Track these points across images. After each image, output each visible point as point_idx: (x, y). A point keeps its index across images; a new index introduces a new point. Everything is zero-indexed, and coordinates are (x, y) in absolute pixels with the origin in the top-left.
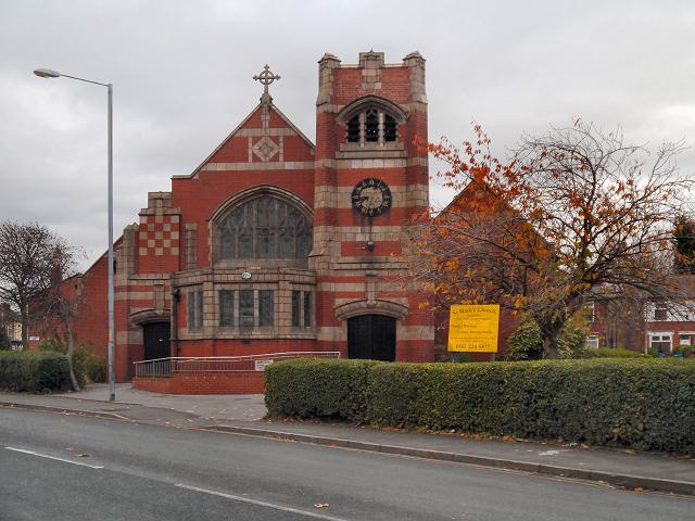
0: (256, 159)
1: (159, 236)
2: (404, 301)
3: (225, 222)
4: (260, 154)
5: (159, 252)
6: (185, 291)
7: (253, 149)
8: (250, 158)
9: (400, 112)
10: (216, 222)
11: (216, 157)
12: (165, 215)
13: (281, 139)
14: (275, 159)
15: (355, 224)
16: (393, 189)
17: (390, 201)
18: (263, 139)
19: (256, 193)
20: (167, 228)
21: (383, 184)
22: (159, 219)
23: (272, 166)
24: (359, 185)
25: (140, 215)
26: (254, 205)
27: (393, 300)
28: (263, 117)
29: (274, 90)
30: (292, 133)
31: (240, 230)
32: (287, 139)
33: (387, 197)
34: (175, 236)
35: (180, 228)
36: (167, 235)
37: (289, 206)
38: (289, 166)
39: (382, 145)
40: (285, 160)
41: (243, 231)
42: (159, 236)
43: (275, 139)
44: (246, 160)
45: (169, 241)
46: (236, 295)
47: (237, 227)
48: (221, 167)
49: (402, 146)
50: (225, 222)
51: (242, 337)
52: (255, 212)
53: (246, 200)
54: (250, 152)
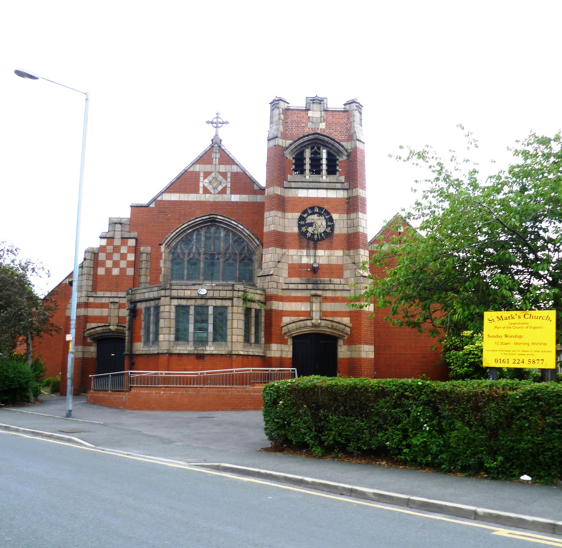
1: (116, 257)
2: (346, 320)
3: (176, 247)
4: (210, 188)
6: (141, 306)
7: (204, 182)
8: (201, 190)
9: (341, 149)
10: (168, 245)
11: (170, 189)
12: (122, 238)
13: (229, 175)
14: (223, 191)
15: (301, 247)
16: (335, 216)
17: (332, 227)
18: (213, 174)
19: (205, 222)
20: (124, 250)
22: (117, 242)
23: (220, 198)
24: (305, 212)
26: (203, 232)
27: (338, 319)
28: (213, 155)
29: (224, 134)
30: (239, 170)
31: (189, 254)
32: (235, 175)
33: (329, 223)
34: (131, 257)
35: (136, 250)
36: (124, 257)
37: (234, 234)
38: (235, 198)
39: (324, 178)
40: (231, 193)
41: (192, 256)
42: (116, 257)
43: (224, 175)
44: (196, 191)
46: (192, 311)
47: (186, 252)
48: (175, 197)
49: (342, 179)
51: (196, 352)
52: (203, 238)
53: (196, 228)
54: (201, 185)
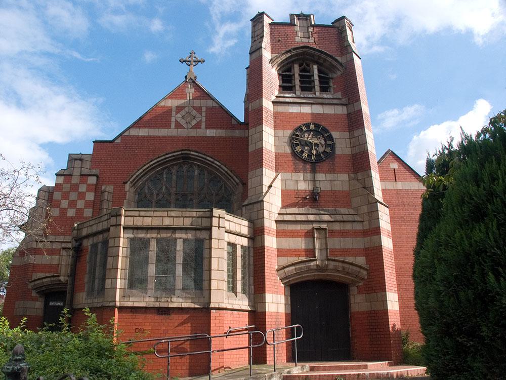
0: (178, 126)
1: (73, 196)
2: (361, 260)
3: (142, 188)
4: (183, 122)
5: (71, 213)
6: (87, 243)
7: (176, 117)
8: (173, 125)
9: (334, 63)
10: (134, 184)
11: (138, 124)
12: (82, 175)
13: (204, 109)
14: (198, 126)
15: (296, 170)
16: (335, 134)
17: (333, 147)
18: (186, 109)
19: (176, 159)
20: (83, 188)
21: (325, 130)
22: (75, 180)
23: (194, 133)
24: (299, 129)
25: (57, 175)
26: (174, 170)
27: (350, 259)
28: (188, 90)
29: (197, 71)
30: (215, 105)
31: (158, 194)
32: (210, 110)
33: (328, 142)
34: (90, 196)
35: (96, 189)
36: (82, 196)
37: (210, 173)
38: (210, 133)
39: (318, 94)
40: (206, 128)
41: (161, 196)
42: (73, 196)
43: (199, 109)
44: (168, 126)
45: (83, 202)
46: (153, 246)
47: (155, 192)
48: (143, 132)
49: (339, 95)
50: (142, 188)
51: (157, 305)
52: (174, 177)
53: (165, 165)
54: (173, 119)
